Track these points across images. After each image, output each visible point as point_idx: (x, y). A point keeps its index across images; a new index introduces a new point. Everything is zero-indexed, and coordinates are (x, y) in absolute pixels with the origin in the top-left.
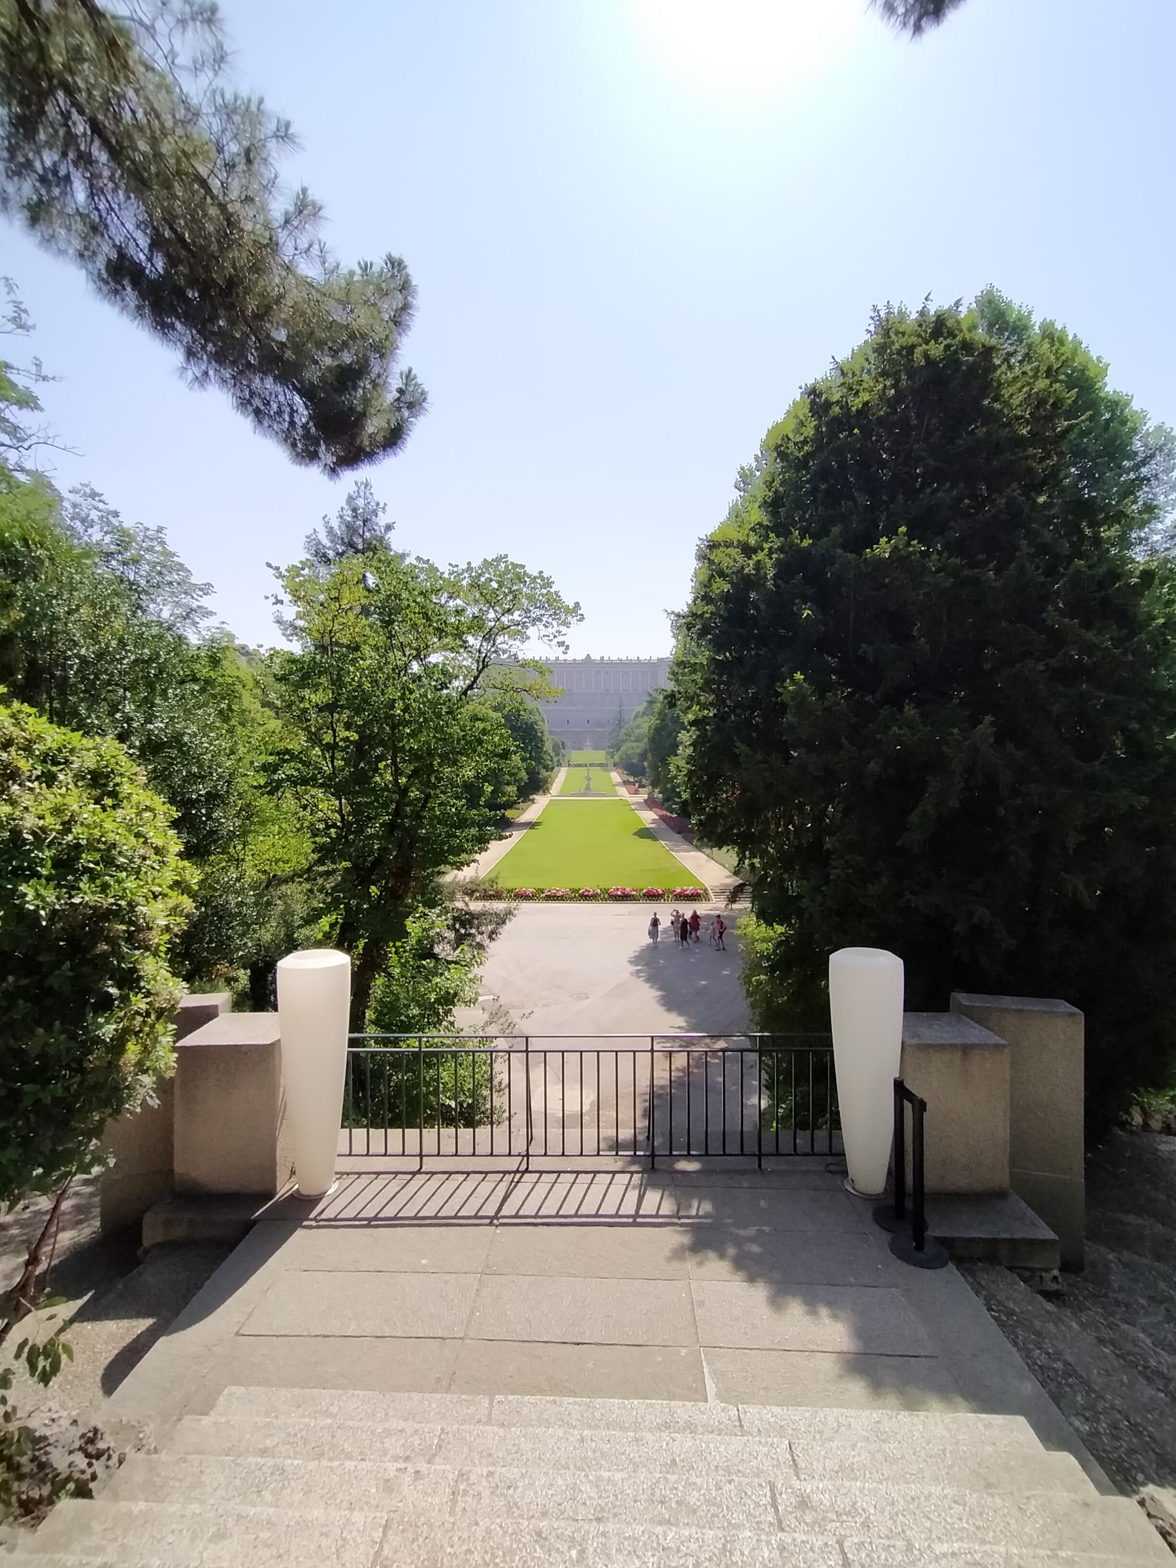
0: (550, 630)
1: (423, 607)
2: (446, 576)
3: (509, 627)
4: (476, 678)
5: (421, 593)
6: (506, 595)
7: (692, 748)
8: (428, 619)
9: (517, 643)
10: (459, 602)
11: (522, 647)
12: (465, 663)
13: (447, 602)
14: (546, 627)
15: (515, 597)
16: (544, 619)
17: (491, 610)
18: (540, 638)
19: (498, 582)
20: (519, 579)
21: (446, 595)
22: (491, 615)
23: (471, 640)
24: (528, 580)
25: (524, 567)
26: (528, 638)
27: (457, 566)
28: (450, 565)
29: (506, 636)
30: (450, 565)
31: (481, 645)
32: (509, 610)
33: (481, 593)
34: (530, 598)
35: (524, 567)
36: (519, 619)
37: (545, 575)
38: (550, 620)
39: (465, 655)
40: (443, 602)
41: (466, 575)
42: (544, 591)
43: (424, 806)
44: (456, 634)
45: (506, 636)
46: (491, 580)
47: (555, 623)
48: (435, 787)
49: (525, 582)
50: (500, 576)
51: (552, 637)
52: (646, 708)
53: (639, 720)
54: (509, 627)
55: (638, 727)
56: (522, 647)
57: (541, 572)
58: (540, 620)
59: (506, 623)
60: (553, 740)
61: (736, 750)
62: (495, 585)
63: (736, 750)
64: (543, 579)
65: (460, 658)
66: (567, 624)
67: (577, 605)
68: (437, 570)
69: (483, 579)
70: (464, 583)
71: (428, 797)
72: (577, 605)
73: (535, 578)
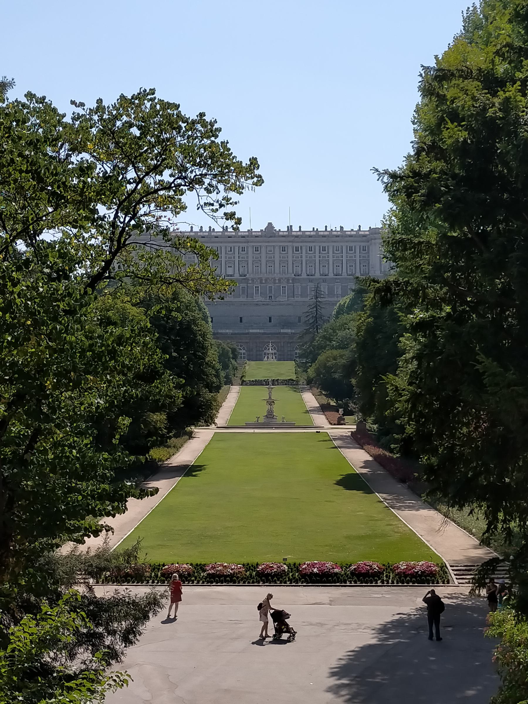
0: (214, 196)
1: (33, 164)
2: (68, 119)
3: (156, 191)
4: (108, 263)
5: (30, 144)
6: (152, 146)
7: (415, 362)
8: (40, 180)
9: (168, 214)
10: (85, 156)
11: (174, 220)
12: (93, 241)
13: (68, 156)
14: (209, 191)
15: (165, 150)
16: (207, 181)
17: (130, 168)
18: (200, 207)
19: (140, 128)
20: (170, 124)
21: (67, 146)
22: (131, 174)
23: (102, 209)
24: (183, 125)
25: (177, 107)
26: (184, 208)
27: (82, 105)
28: (73, 102)
29: (153, 205)
30: (73, 102)
31: (116, 216)
32: (156, 167)
33: (117, 143)
34: (186, 151)
35: (177, 107)
36: (171, 180)
37: (208, 118)
38: (214, 183)
39: (93, 231)
40: (63, 154)
41: (96, 118)
42: (206, 142)
43: (30, 447)
44: (80, 202)
45: (153, 205)
46: (131, 125)
47: (221, 187)
48: (48, 419)
49: (180, 128)
50: (143, 120)
51: (216, 206)
52: (353, 302)
53: (345, 317)
54: (156, 191)
55: (344, 326)
56: (174, 220)
57: (202, 115)
58: (200, 182)
59: (152, 185)
60: (219, 346)
61: (478, 367)
62: (135, 131)
63: (478, 367)
64: (204, 124)
65: (86, 235)
66: (238, 190)
67: (254, 163)
68: (55, 110)
69: (119, 123)
70: (94, 131)
71: (37, 432)
72: (254, 163)
73: (194, 122)
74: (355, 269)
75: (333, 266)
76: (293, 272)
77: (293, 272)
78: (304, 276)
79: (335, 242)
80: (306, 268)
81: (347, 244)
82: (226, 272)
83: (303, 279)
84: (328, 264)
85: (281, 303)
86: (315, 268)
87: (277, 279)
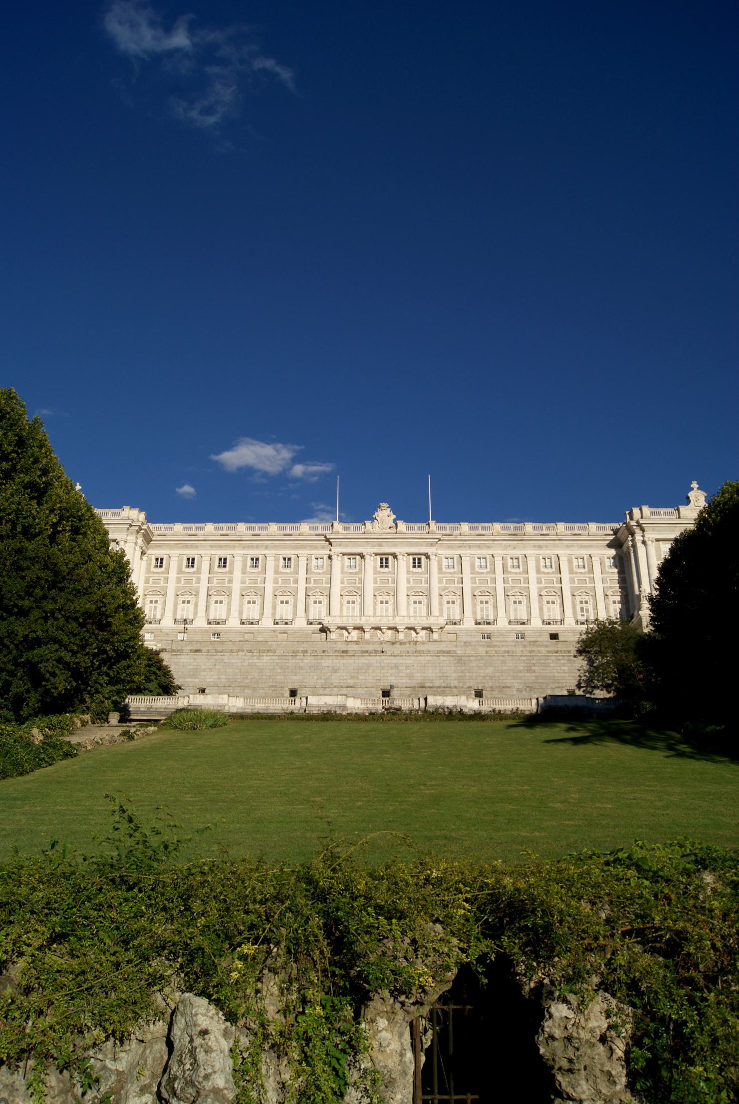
74: (596, 608)
75: (540, 602)
76: (441, 615)
79: (540, 547)
80: (474, 606)
81: (568, 552)
82: (274, 614)
83: (468, 632)
84: (528, 597)
85: (420, 647)
86: (496, 607)
87: (401, 628)
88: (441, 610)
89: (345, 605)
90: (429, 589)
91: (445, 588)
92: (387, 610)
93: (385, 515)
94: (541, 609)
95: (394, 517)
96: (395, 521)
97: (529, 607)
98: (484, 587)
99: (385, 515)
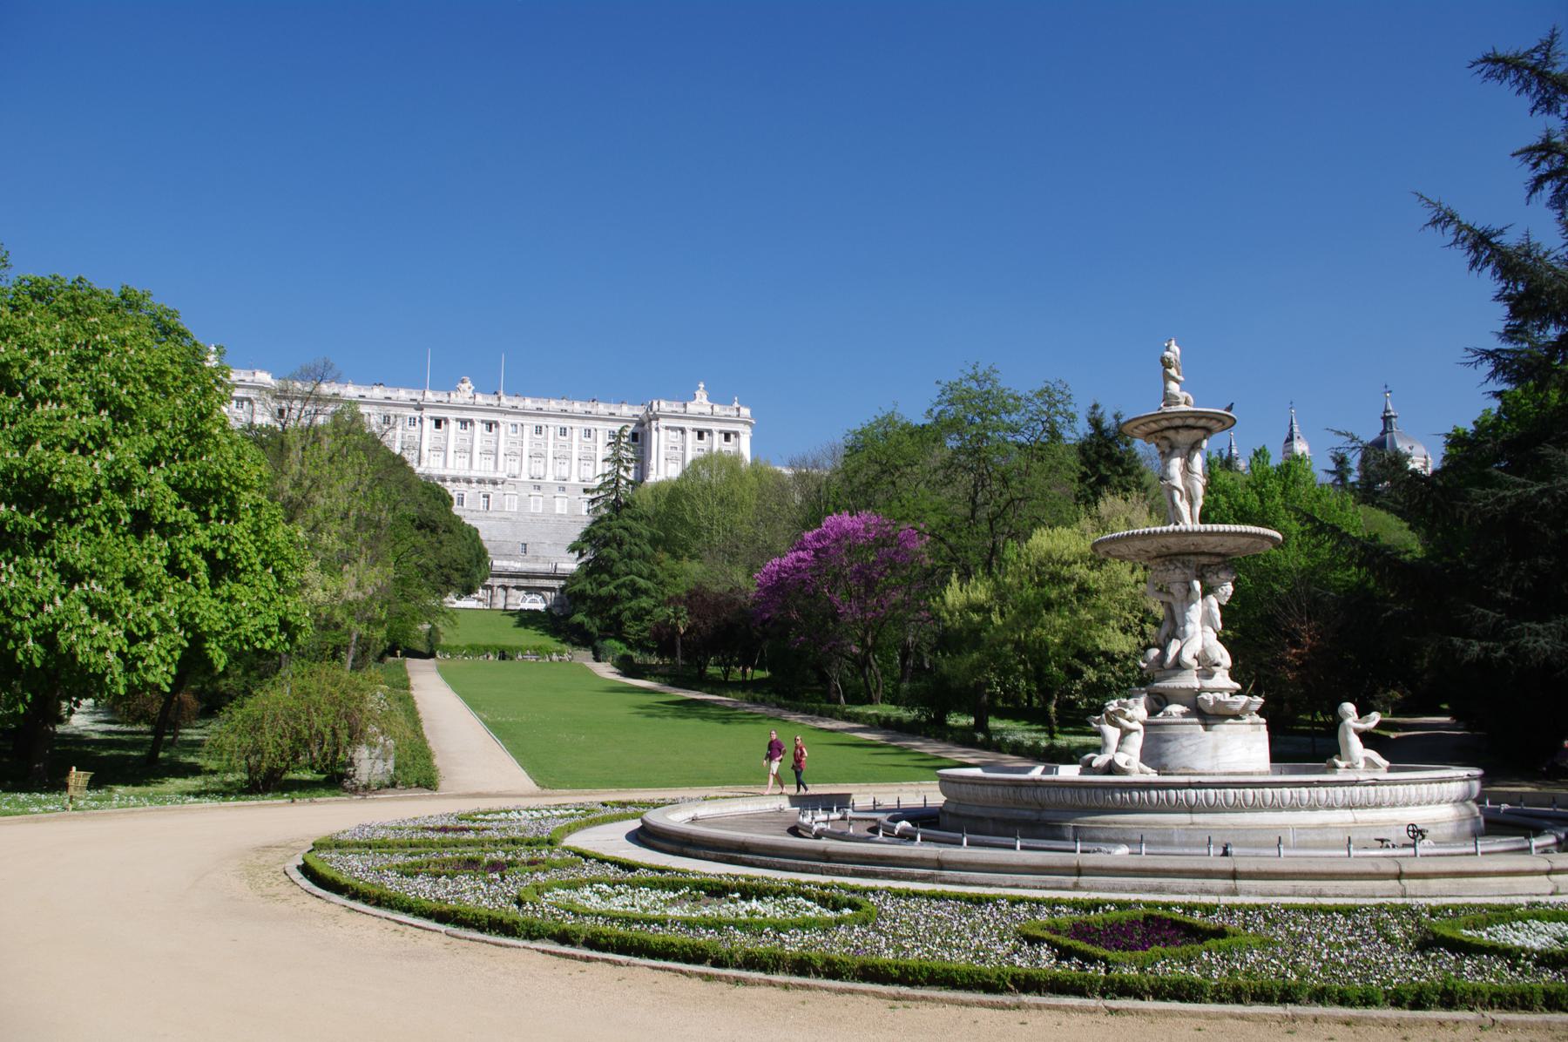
75: (579, 464)
77: (505, 471)
78: (525, 477)
86: (546, 466)
87: (474, 480)
88: (505, 466)
89: (432, 458)
90: (497, 449)
91: (509, 449)
92: (464, 463)
93: (467, 387)
94: (579, 470)
95: (473, 388)
96: (474, 391)
97: (570, 467)
98: (539, 450)
99: (467, 387)
